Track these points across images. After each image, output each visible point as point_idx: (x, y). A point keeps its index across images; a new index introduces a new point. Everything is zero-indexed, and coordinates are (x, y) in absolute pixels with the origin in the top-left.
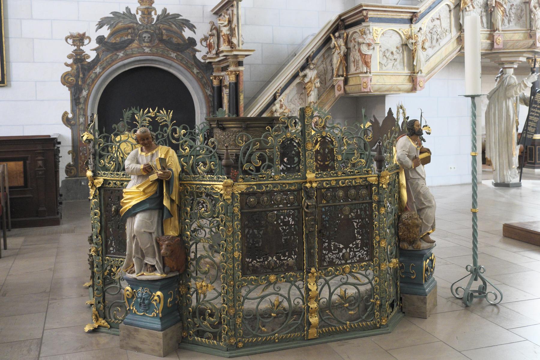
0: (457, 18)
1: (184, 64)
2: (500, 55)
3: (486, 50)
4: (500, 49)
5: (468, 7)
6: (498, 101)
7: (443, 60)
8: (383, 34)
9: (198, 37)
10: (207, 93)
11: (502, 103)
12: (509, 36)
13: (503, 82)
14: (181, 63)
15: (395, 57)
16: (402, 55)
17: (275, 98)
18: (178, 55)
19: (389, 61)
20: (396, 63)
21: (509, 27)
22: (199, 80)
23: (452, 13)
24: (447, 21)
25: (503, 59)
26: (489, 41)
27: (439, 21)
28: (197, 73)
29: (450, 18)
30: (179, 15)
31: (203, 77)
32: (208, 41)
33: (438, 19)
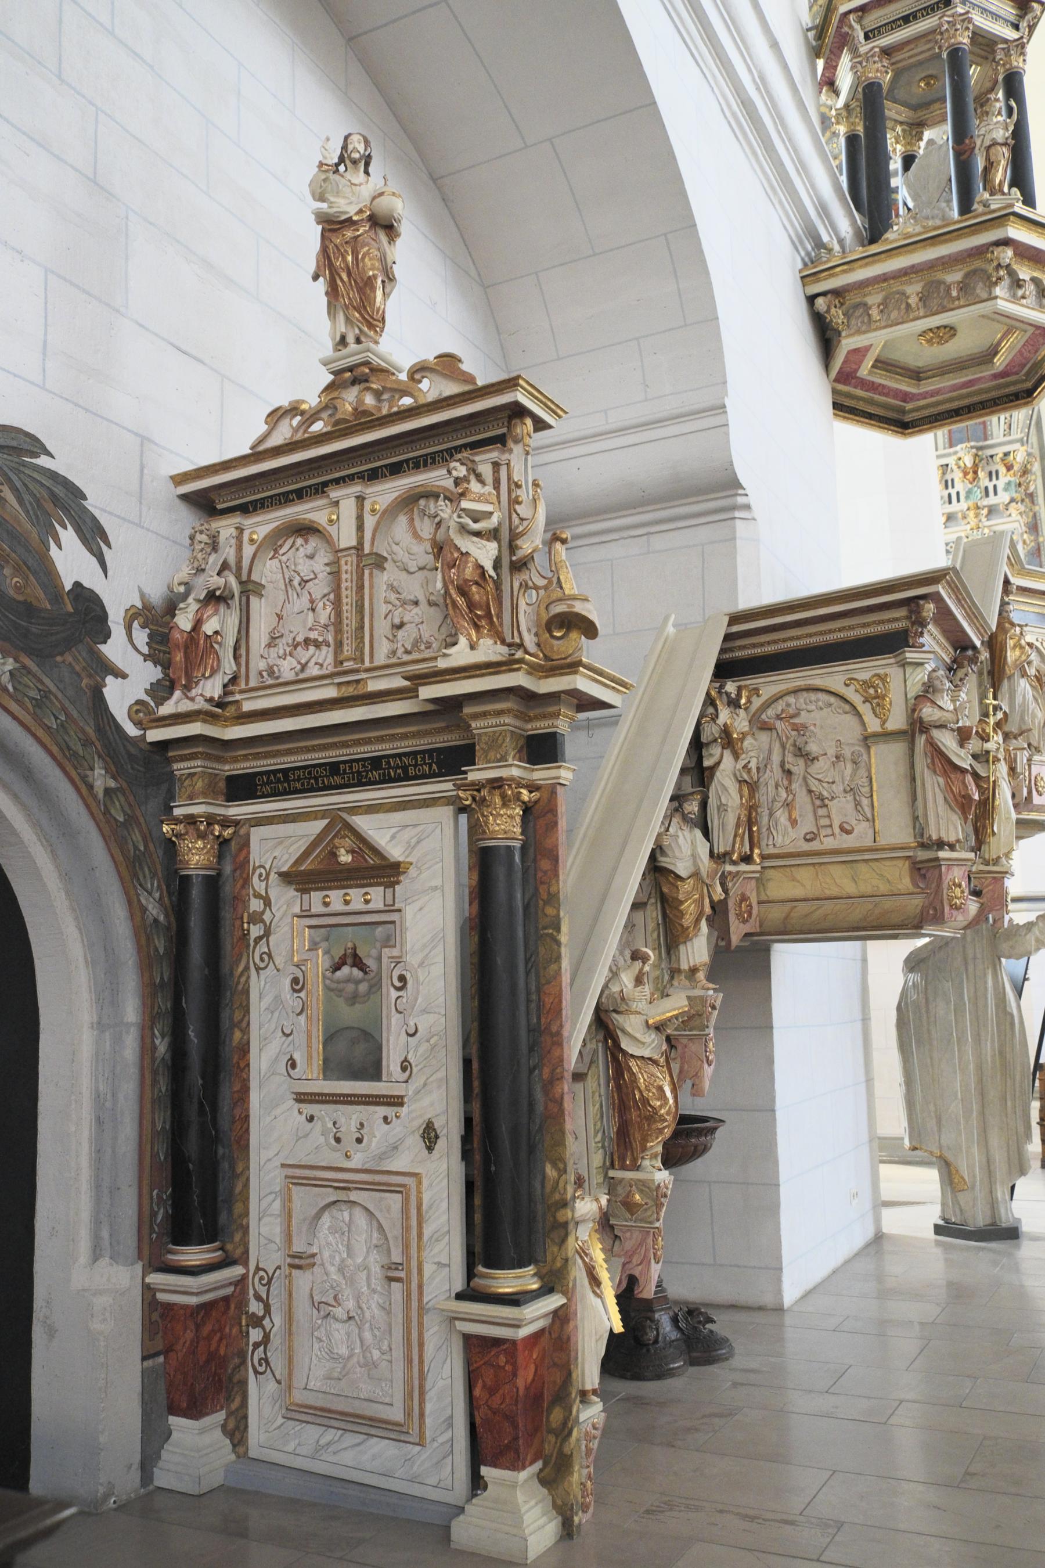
1: (48, 729)
9: (117, 598)
10: (144, 910)
14: (35, 717)
18: (29, 672)
22: (115, 835)
28: (107, 791)
30: (37, 447)
31: (131, 820)
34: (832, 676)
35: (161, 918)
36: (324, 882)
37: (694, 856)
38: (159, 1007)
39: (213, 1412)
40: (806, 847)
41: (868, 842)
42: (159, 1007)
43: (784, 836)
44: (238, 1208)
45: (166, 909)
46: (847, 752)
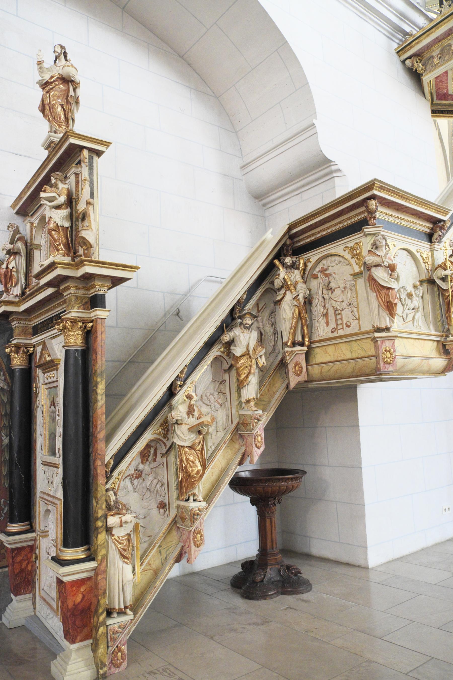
17: (171, 392)
32: (4, 266)
34: (337, 247)
35: (6, 387)
36: (47, 369)
37: (248, 346)
38: (4, 424)
39: (25, 594)
40: (331, 335)
41: (356, 331)
42: (4, 424)
43: (322, 330)
44: (35, 507)
45: (8, 383)
46: (348, 286)
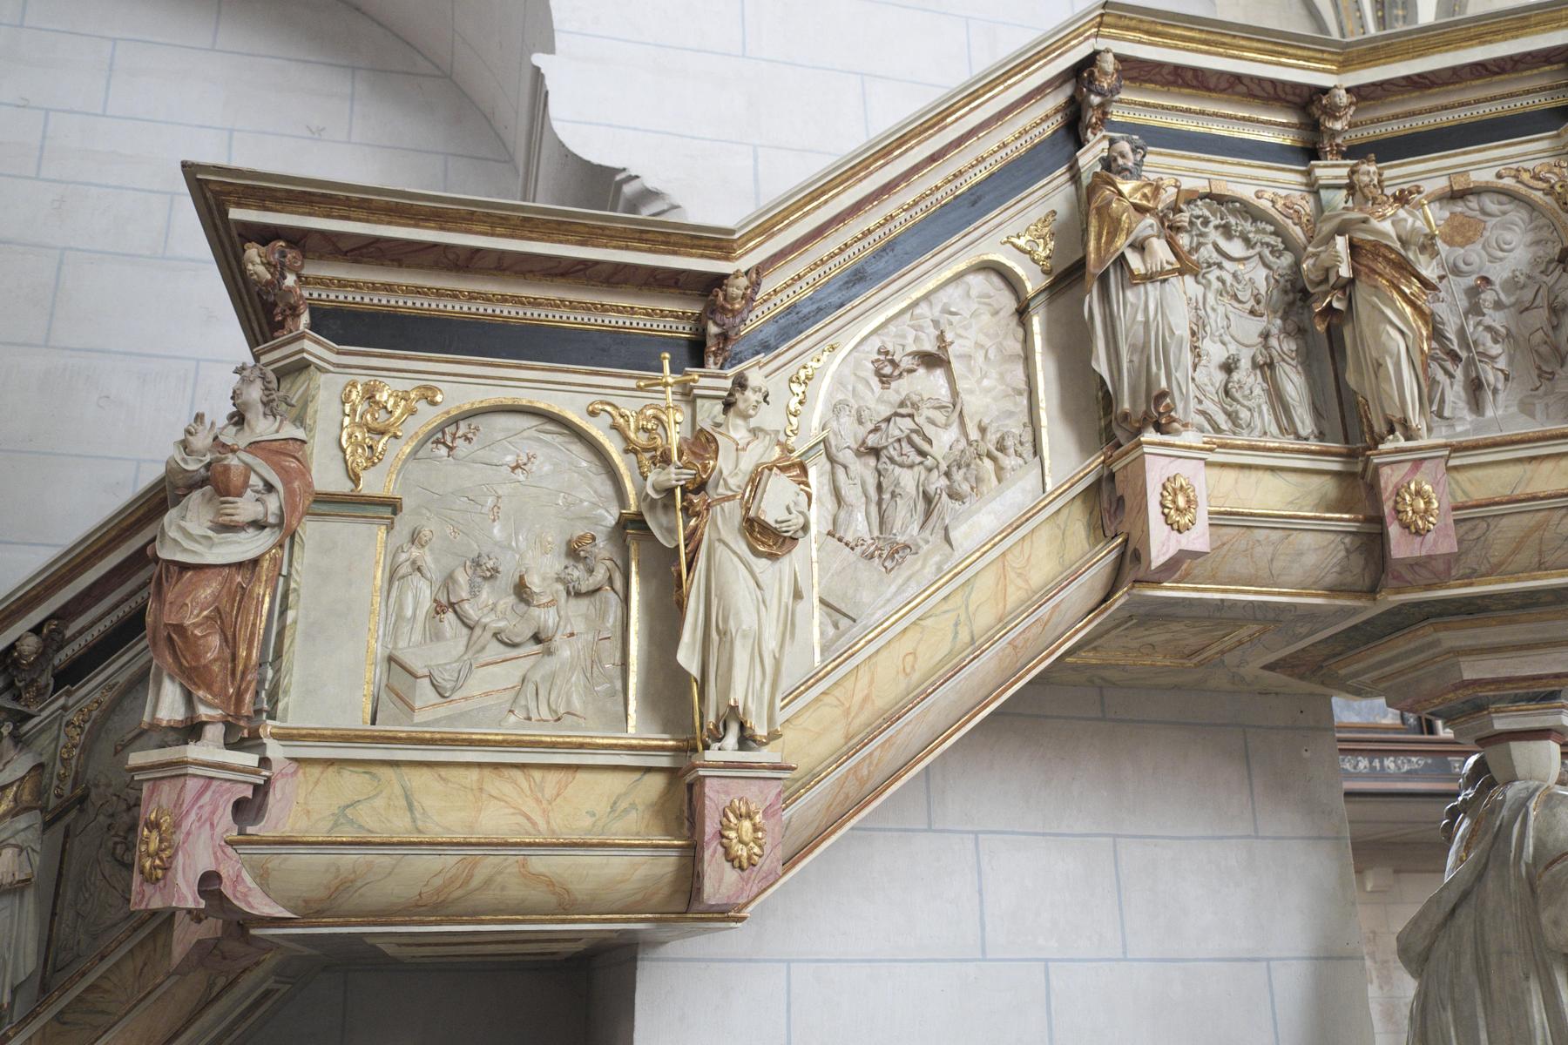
0: (1073, 348)
2: (1451, 638)
3: (1333, 591)
4: (1428, 569)
5: (1140, 247)
6: (1484, 983)
7: (976, 649)
8: (440, 435)
11: (1519, 1004)
12: (1492, 481)
13: (1502, 834)
15: (547, 618)
16: (614, 600)
19: (495, 650)
20: (551, 664)
21: (1476, 430)
23: (1037, 323)
24: (997, 375)
25: (1472, 670)
26: (1345, 520)
27: (939, 373)
29: (1028, 359)
33: (932, 360)
